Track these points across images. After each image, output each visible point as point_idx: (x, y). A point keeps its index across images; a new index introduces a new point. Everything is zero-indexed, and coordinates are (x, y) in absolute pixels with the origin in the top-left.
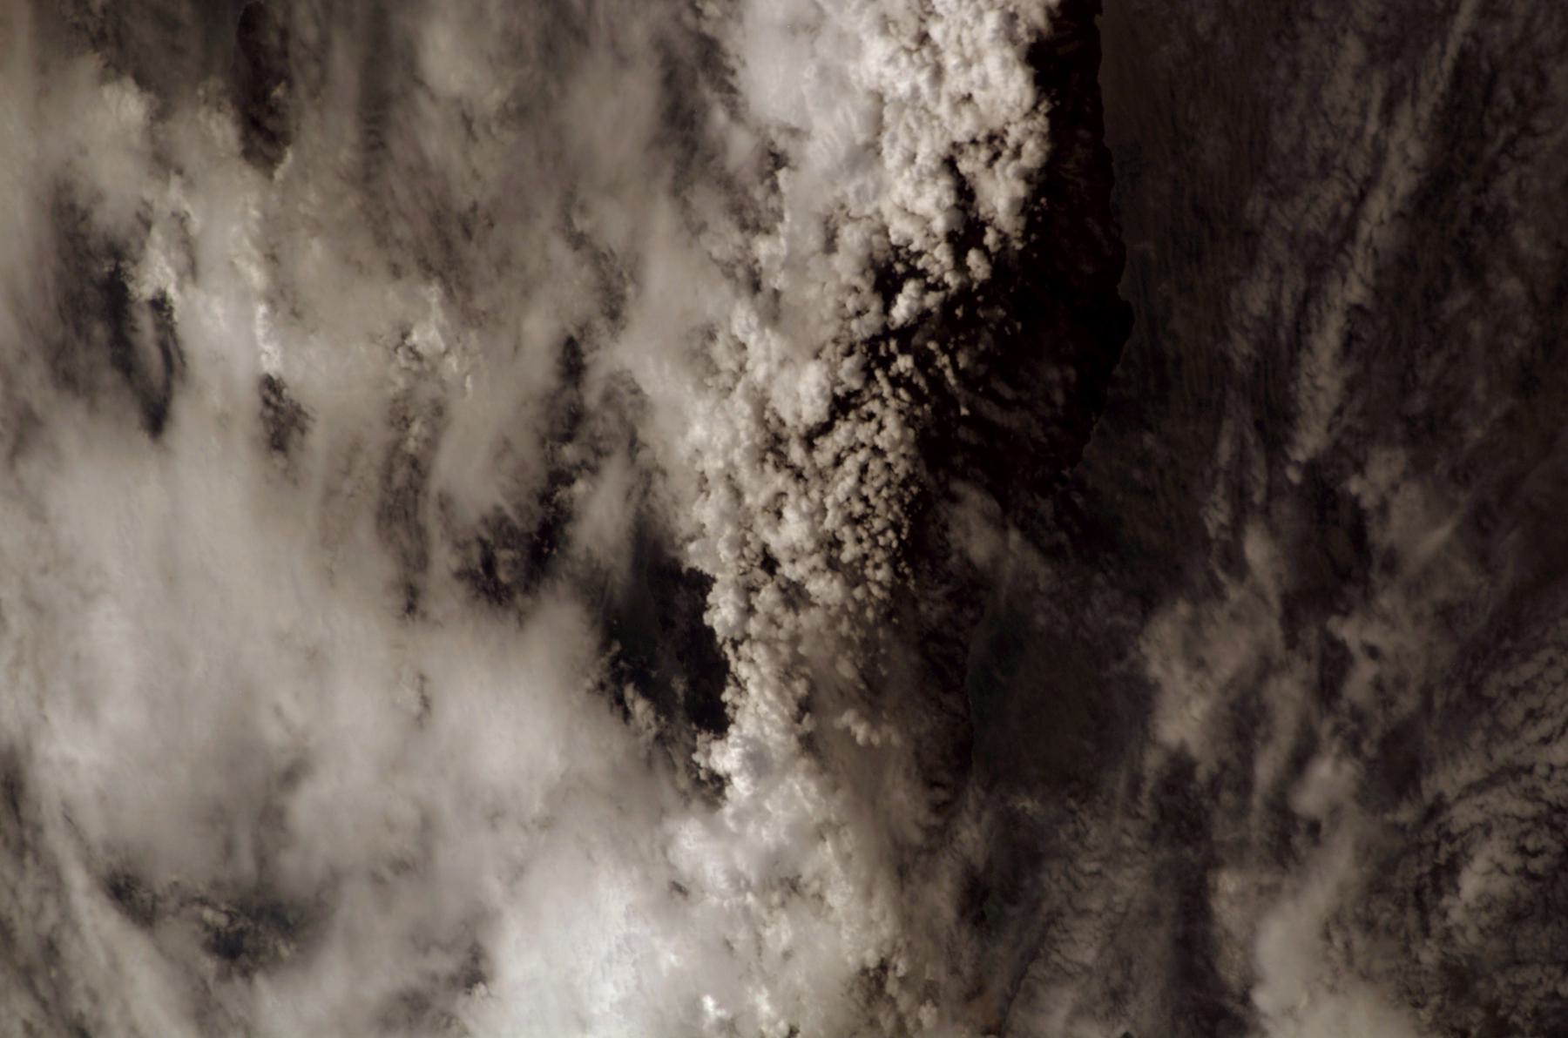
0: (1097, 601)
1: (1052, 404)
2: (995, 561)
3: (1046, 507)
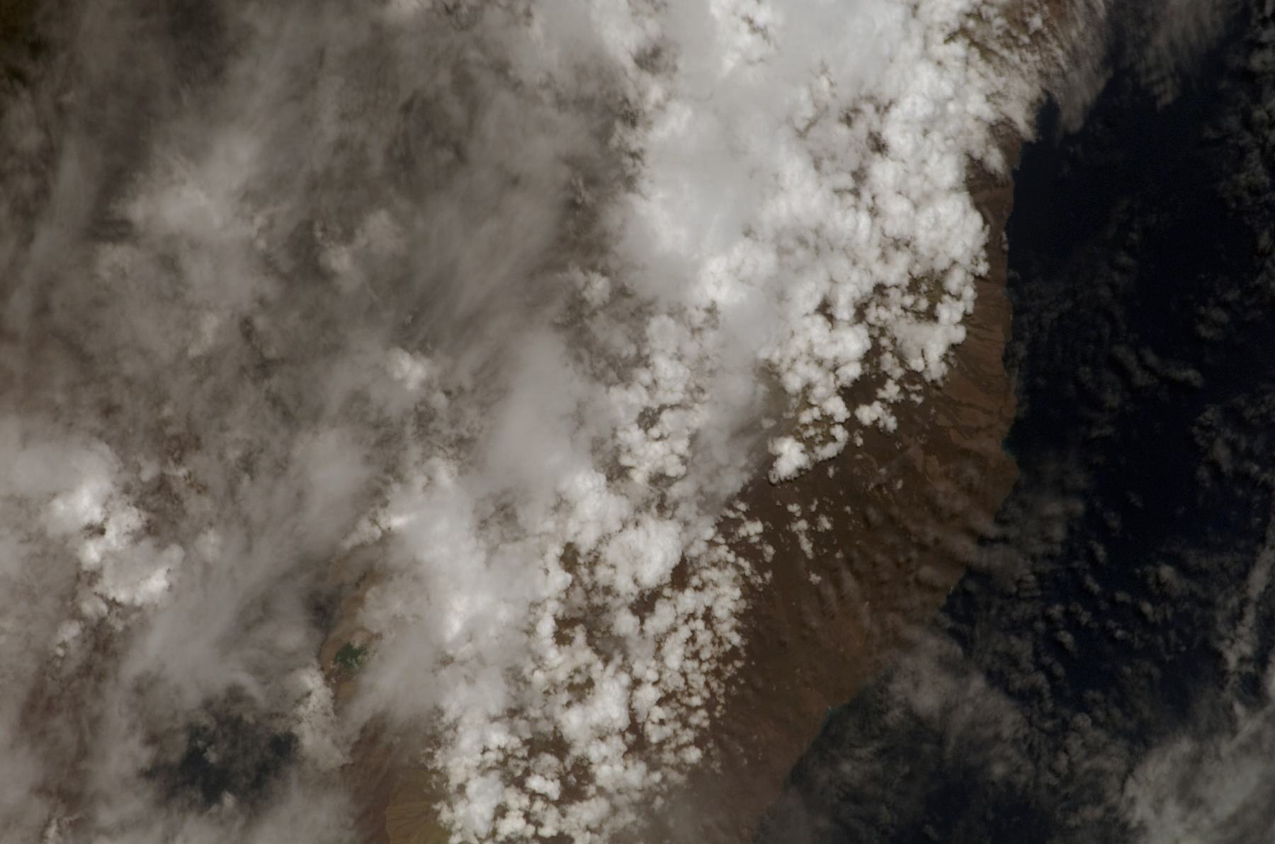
0: (1074, 743)
1: (1047, 540)
2: (947, 710)
3: (1023, 647)
